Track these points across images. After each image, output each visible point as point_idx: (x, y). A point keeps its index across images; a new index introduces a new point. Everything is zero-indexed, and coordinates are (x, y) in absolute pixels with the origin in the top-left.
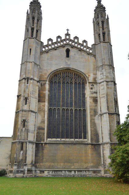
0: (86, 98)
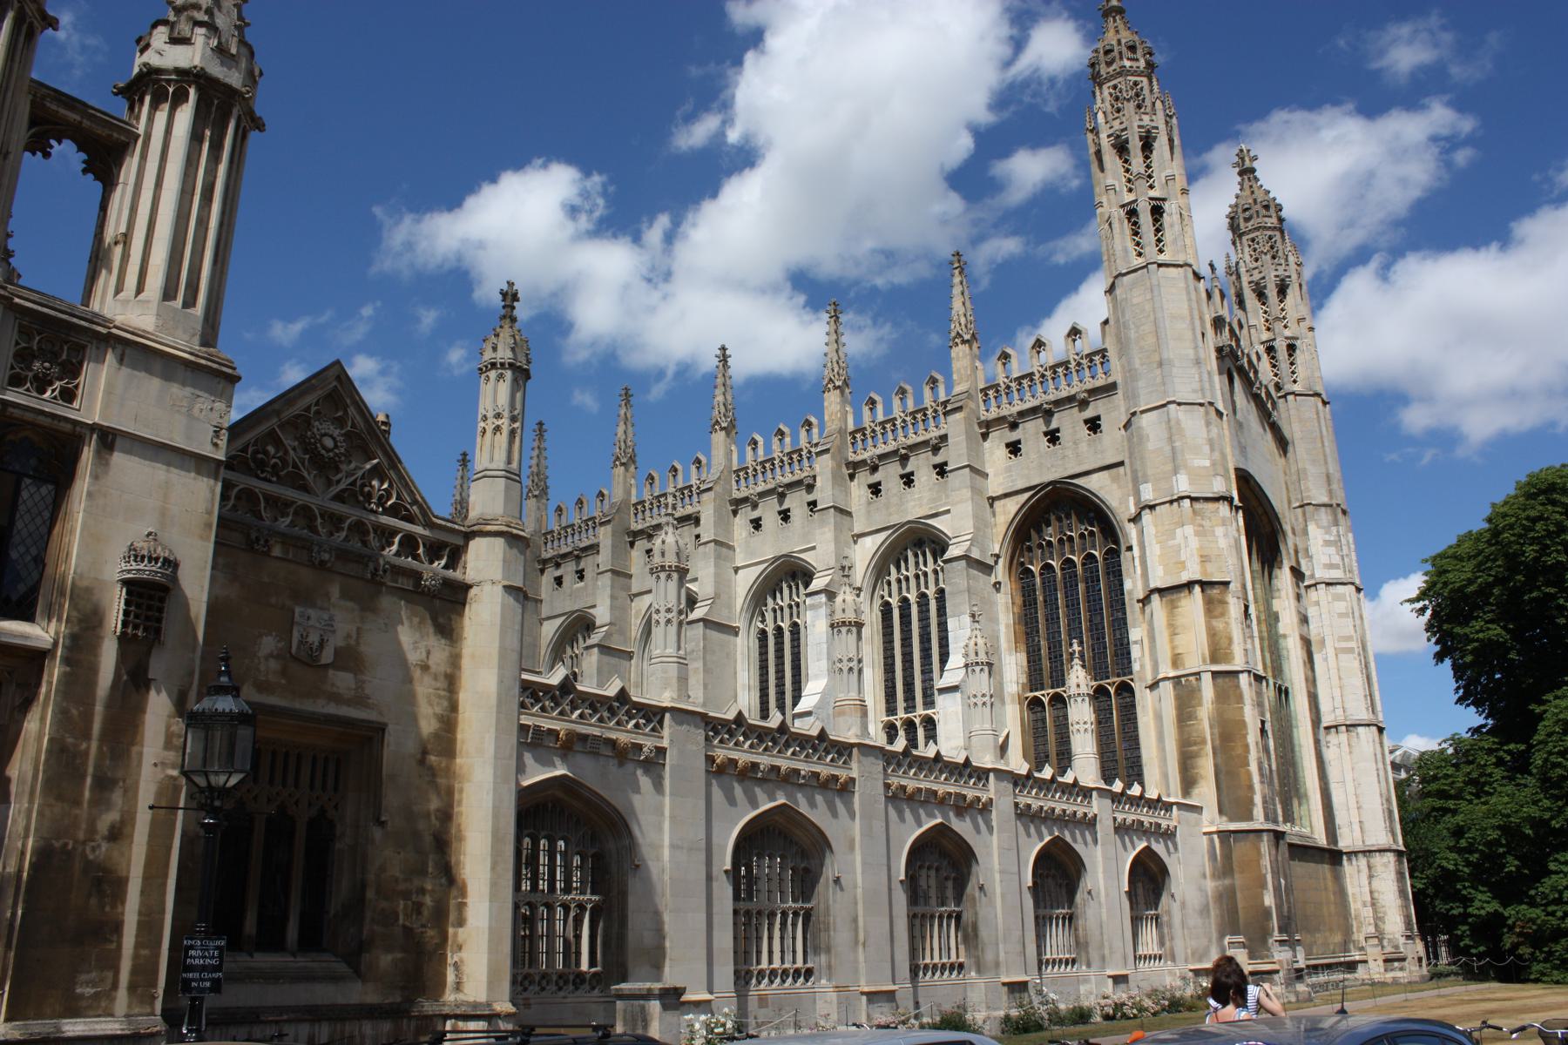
0: (1285, 636)
